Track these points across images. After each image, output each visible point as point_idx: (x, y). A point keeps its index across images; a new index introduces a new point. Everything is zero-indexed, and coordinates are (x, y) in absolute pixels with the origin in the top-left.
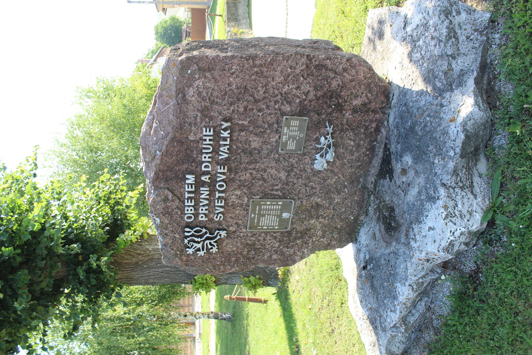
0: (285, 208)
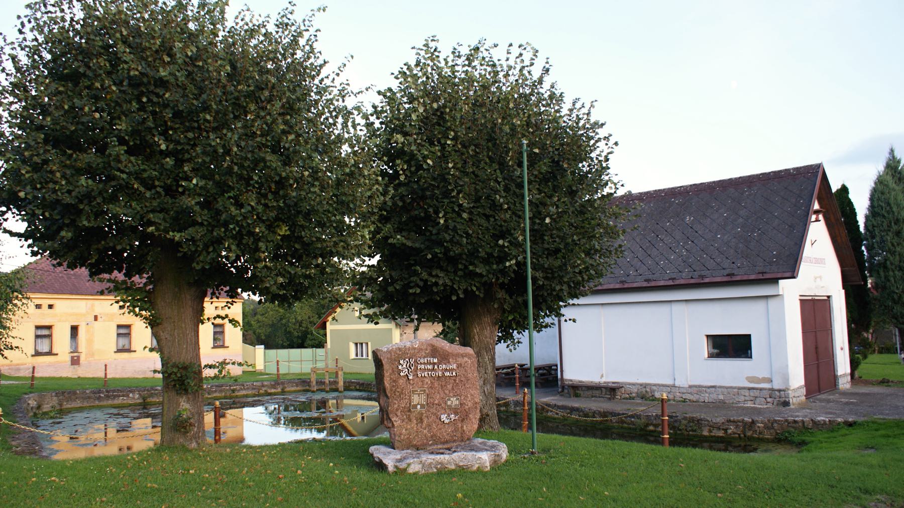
0: (422, 406)
